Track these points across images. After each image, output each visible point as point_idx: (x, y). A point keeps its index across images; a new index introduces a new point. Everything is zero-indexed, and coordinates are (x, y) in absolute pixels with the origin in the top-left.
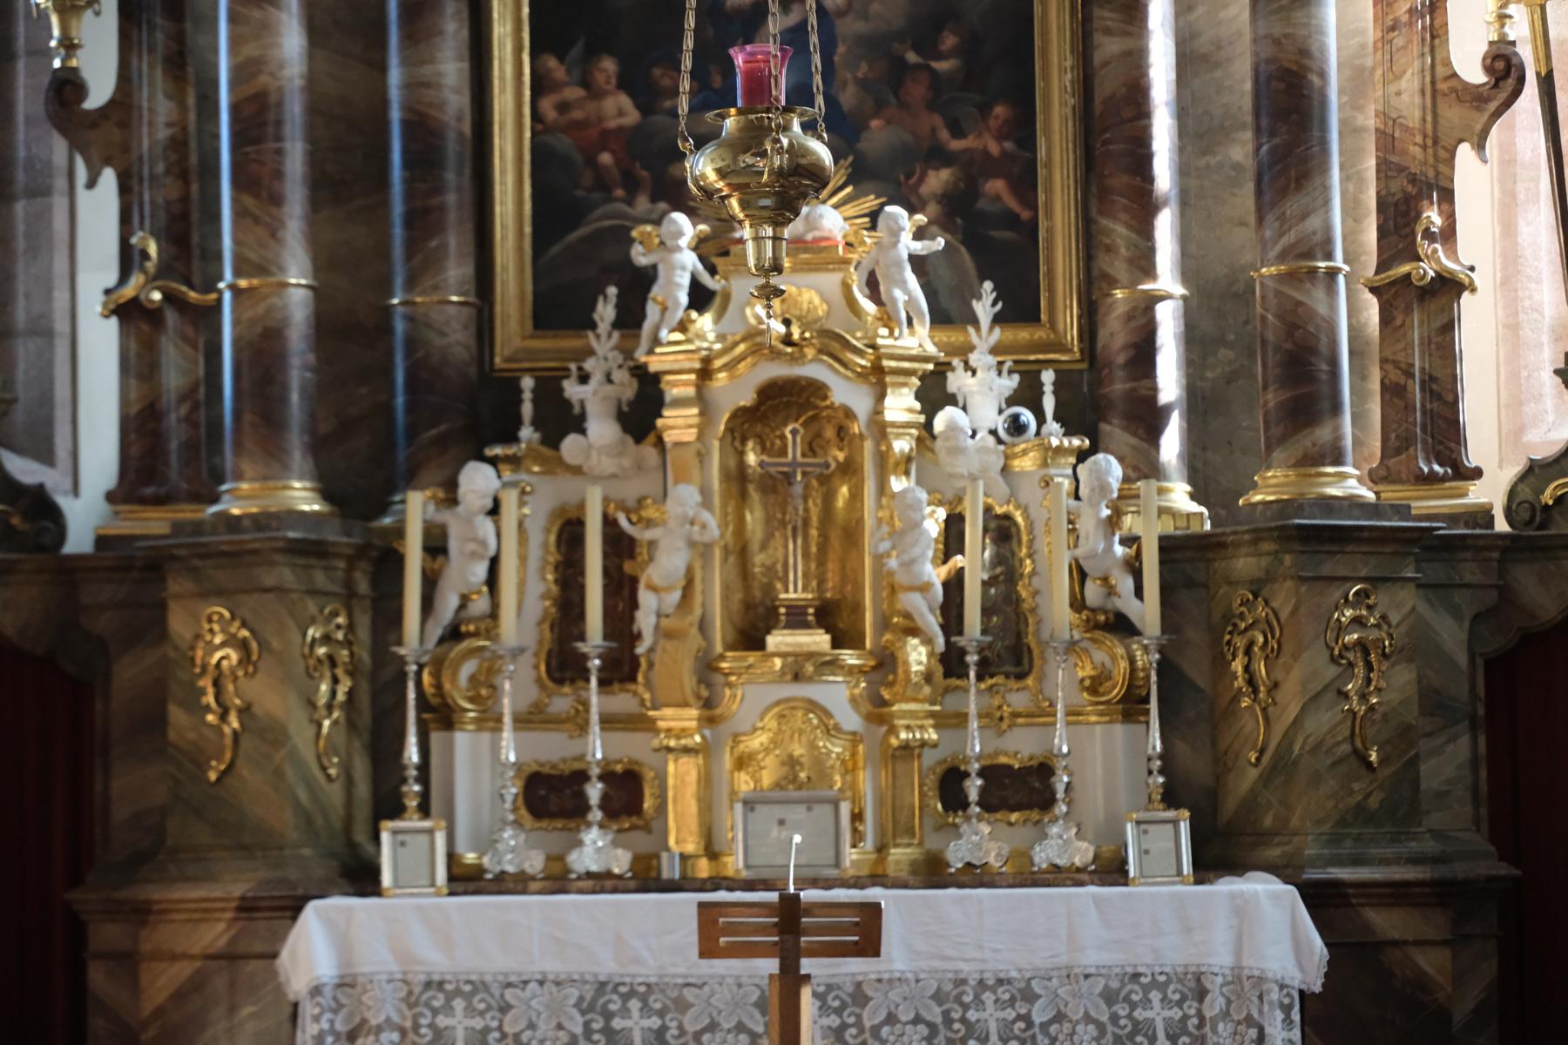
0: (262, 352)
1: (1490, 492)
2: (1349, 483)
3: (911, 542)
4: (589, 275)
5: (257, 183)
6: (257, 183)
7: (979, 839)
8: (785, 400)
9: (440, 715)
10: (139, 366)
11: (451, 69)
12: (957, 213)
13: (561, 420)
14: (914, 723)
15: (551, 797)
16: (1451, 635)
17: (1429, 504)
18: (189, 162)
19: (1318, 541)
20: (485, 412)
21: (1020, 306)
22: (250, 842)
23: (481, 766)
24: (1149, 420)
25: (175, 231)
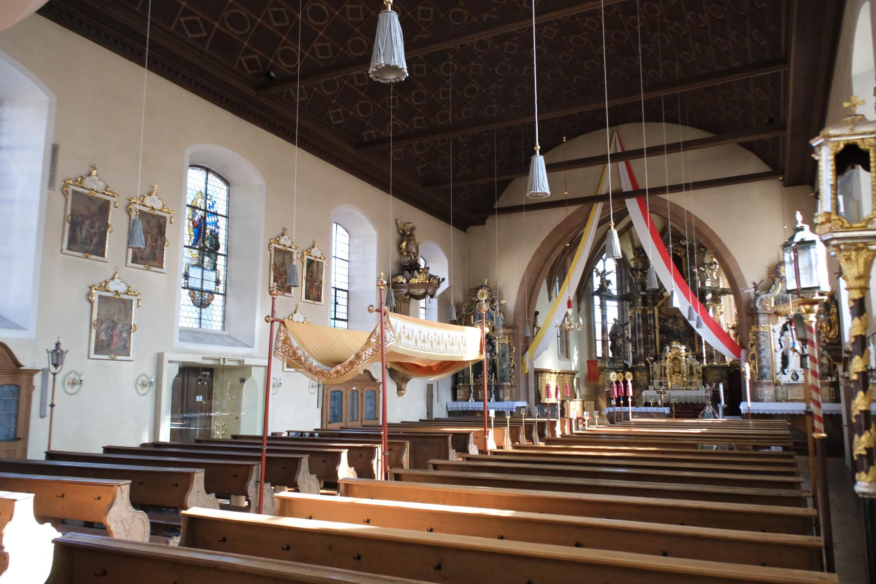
0: (640, 355)
1: (728, 364)
2: (715, 363)
3: (684, 366)
4: (662, 350)
5: (640, 345)
6: (640, 345)
7: (689, 387)
8: (675, 358)
9: (653, 379)
10: (633, 356)
11: (653, 336)
12: (690, 344)
13: (661, 359)
14: (685, 379)
15: (661, 384)
16: (725, 373)
17: (721, 364)
18: (635, 342)
19: (713, 368)
20: (657, 358)
21: (694, 350)
22: (640, 387)
23: (656, 382)
24: (702, 358)
25: (635, 346)
